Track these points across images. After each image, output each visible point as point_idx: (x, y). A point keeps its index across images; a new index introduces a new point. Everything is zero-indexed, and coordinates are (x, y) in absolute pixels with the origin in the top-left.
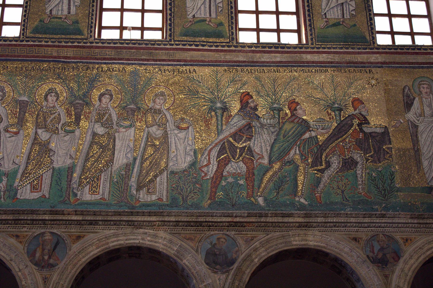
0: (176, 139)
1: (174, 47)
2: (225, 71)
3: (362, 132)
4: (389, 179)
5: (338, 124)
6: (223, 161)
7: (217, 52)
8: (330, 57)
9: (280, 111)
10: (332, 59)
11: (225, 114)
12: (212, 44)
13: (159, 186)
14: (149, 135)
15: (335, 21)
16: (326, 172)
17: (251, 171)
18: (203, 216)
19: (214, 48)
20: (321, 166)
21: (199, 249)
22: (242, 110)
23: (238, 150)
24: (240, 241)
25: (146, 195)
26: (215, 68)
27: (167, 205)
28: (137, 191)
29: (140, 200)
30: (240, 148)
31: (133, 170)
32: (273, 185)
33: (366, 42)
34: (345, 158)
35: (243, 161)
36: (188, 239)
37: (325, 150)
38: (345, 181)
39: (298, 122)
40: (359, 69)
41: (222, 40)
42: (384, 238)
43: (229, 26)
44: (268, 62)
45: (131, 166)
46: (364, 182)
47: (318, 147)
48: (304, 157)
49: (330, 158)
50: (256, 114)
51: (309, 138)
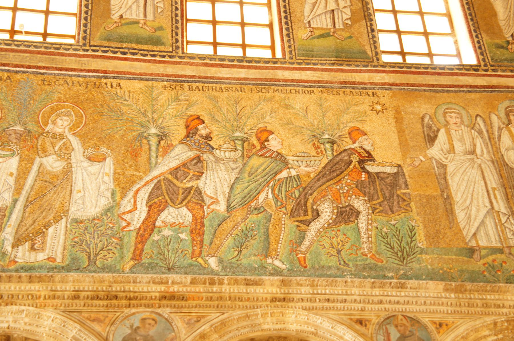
0: (85, 174)
1: (90, 53)
2: (165, 87)
3: (364, 172)
4: (407, 236)
5: (331, 160)
6: (157, 206)
7: (154, 63)
8: (317, 75)
9: (244, 142)
10: (319, 77)
11: (162, 143)
12: (146, 53)
13: (52, 239)
14: (42, 168)
15: (323, 32)
16: (311, 224)
17: (199, 221)
18: (121, 282)
19: (149, 58)
20: (305, 215)
21: (111, 336)
22: (188, 139)
23: (181, 191)
24: (179, 323)
25: (27, 253)
26: (150, 83)
27: (63, 268)
28: (13, 247)
29: (16, 260)
30: (183, 188)
31: (9, 217)
32: (233, 241)
33: (366, 58)
34: (341, 206)
35: (186, 206)
36: (93, 321)
37: (311, 194)
38: (341, 237)
39: (270, 156)
40: (358, 91)
41: (162, 48)
42: (404, 321)
43: (172, 31)
44: (227, 79)
45: (8, 210)
46: (370, 239)
47: (301, 190)
48: (279, 204)
49: (319, 205)
50: (209, 145)
51: (287, 178)
